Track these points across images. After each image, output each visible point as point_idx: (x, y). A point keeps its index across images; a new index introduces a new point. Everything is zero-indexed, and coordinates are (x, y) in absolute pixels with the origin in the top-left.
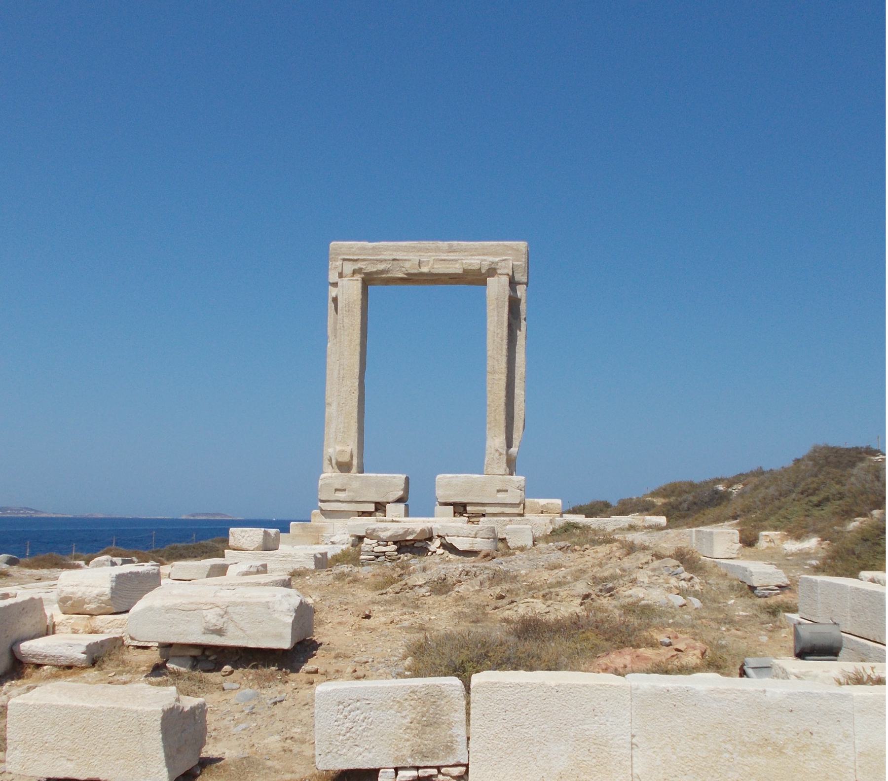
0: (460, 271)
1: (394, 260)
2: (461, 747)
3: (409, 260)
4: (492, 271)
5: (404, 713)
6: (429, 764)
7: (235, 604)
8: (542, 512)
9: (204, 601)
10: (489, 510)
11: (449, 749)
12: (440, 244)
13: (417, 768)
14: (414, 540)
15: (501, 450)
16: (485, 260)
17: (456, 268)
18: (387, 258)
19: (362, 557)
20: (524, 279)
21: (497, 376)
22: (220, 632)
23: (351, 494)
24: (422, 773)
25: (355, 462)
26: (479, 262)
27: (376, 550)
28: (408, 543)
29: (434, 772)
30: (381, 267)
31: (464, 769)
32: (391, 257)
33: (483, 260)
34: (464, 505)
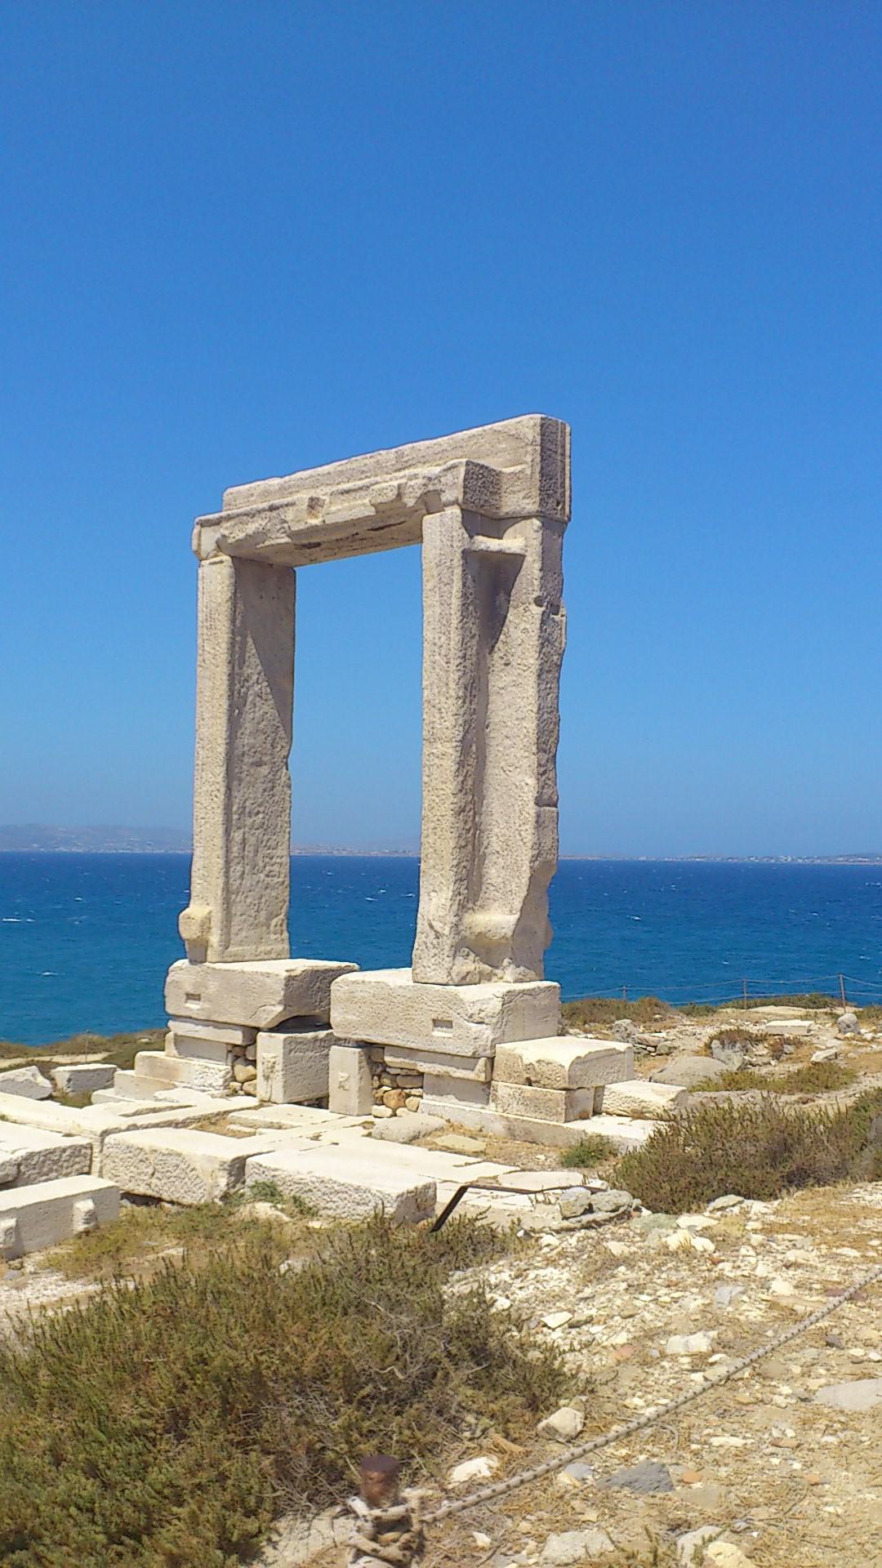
0: (371, 511)
1: (272, 508)
3: (293, 504)
4: (430, 502)
8: (529, 1082)
12: (387, 456)
15: (437, 925)
16: (416, 476)
17: (359, 508)
18: (261, 506)
20: (531, 506)
21: (440, 748)
23: (207, 1006)
25: (215, 939)
26: (395, 483)
30: (252, 527)
32: (266, 505)
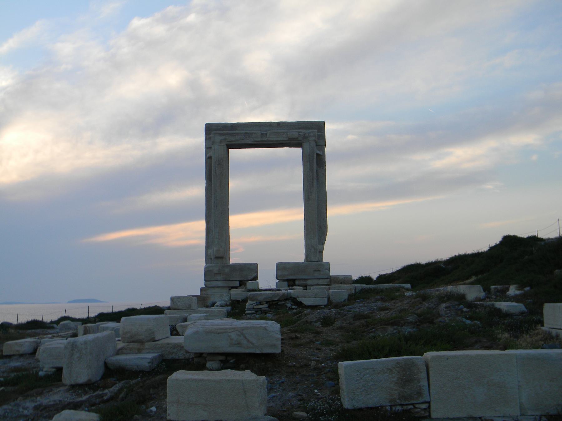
2: (426, 392)
5: (394, 375)
6: (407, 402)
7: (247, 328)
9: (227, 327)
10: (309, 282)
11: (420, 394)
13: (402, 405)
14: (278, 300)
16: (301, 132)
18: (242, 132)
19: (247, 312)
22: (239, 344)
24: (405, 408)
27: (256, 307)
28: (274, 303)
29: (411, 407)
31: (427, 405)
33: (299, 132)
34: (294, 280)
